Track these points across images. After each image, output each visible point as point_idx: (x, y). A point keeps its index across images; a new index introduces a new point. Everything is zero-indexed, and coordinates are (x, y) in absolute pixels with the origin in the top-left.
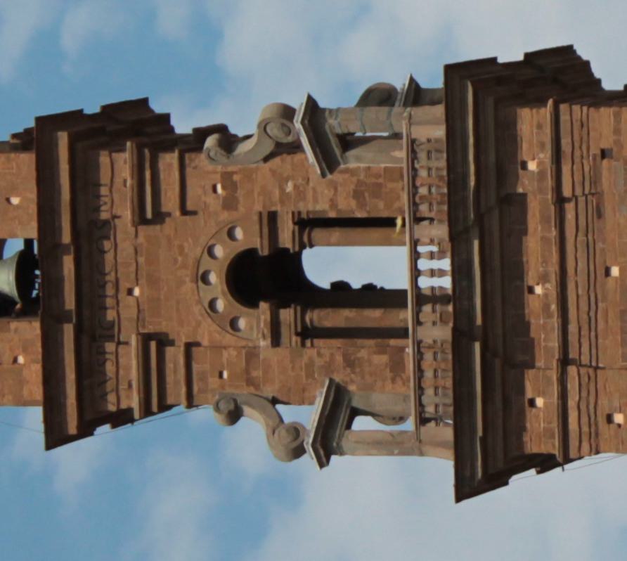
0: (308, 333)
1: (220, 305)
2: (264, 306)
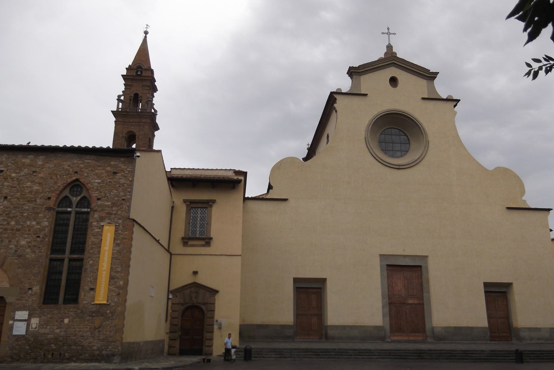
0: (130, 100)
1: (134, 92)
2: (133, 96)
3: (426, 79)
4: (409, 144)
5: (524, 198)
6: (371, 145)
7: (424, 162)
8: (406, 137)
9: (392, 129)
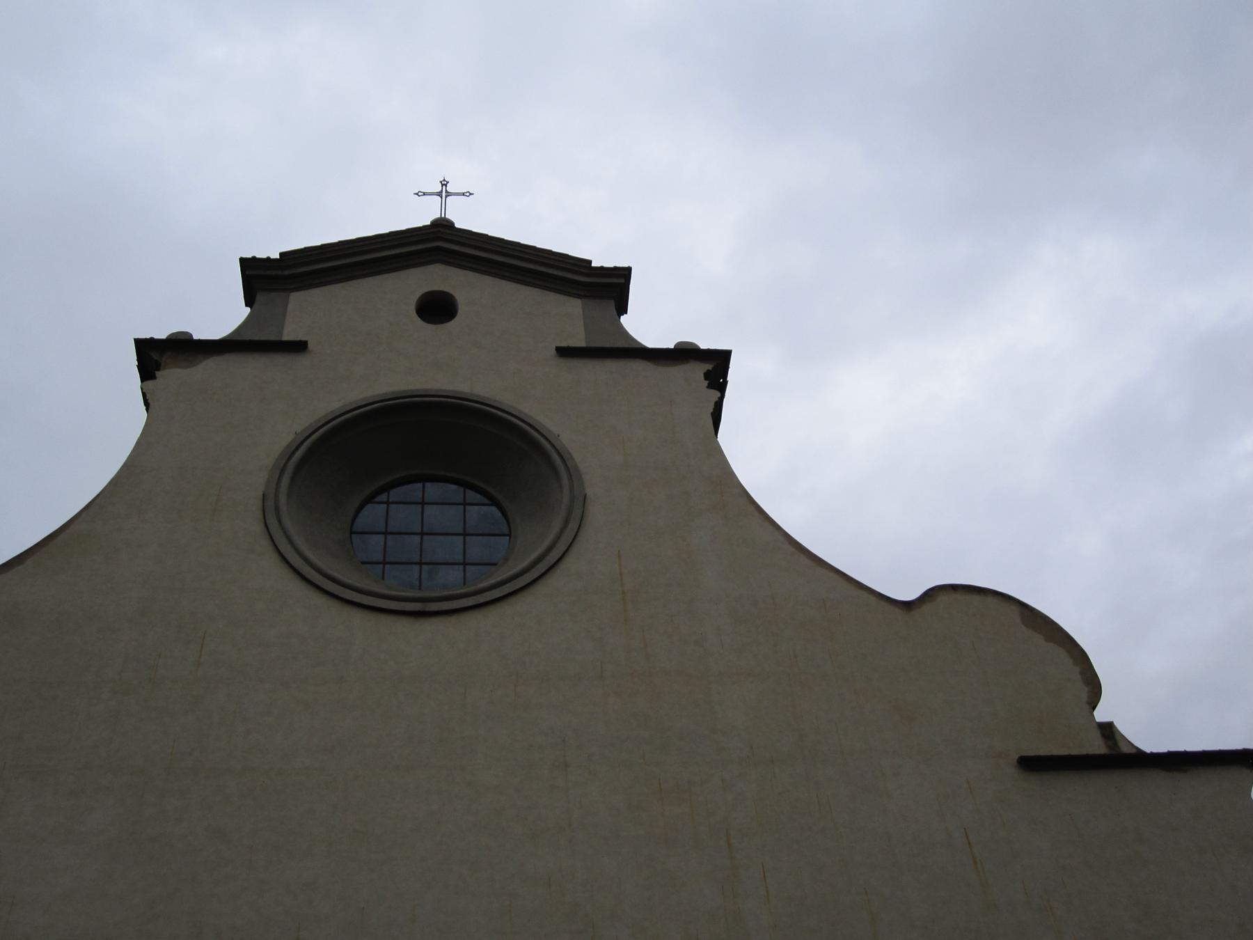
3: (578, 296)
4: (509, 535)
5: (1101, 715)
6: (287, 522)
7: (555, 582)
8: (494, 509)
9: (428, 484)
